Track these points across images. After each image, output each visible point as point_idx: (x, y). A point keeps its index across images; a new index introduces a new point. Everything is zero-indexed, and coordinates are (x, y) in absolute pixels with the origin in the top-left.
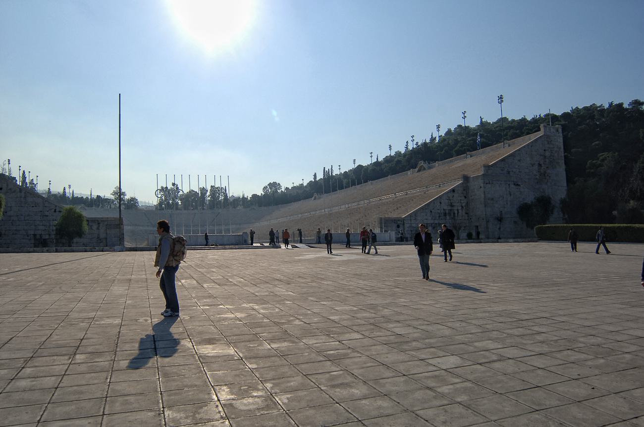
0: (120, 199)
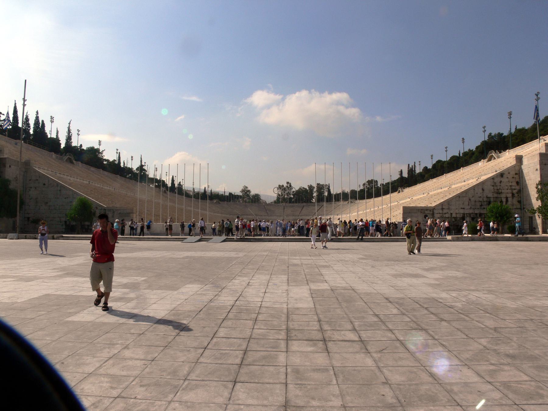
0: (248, 196)
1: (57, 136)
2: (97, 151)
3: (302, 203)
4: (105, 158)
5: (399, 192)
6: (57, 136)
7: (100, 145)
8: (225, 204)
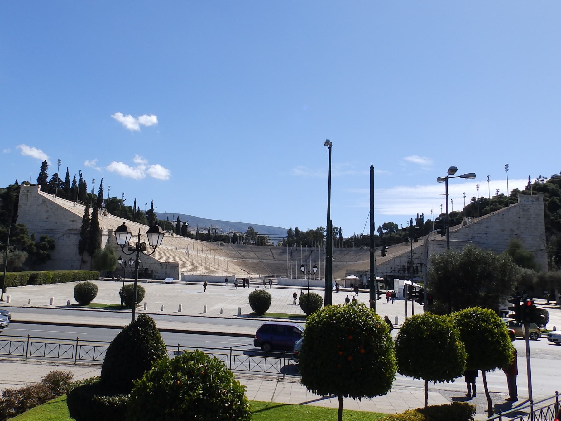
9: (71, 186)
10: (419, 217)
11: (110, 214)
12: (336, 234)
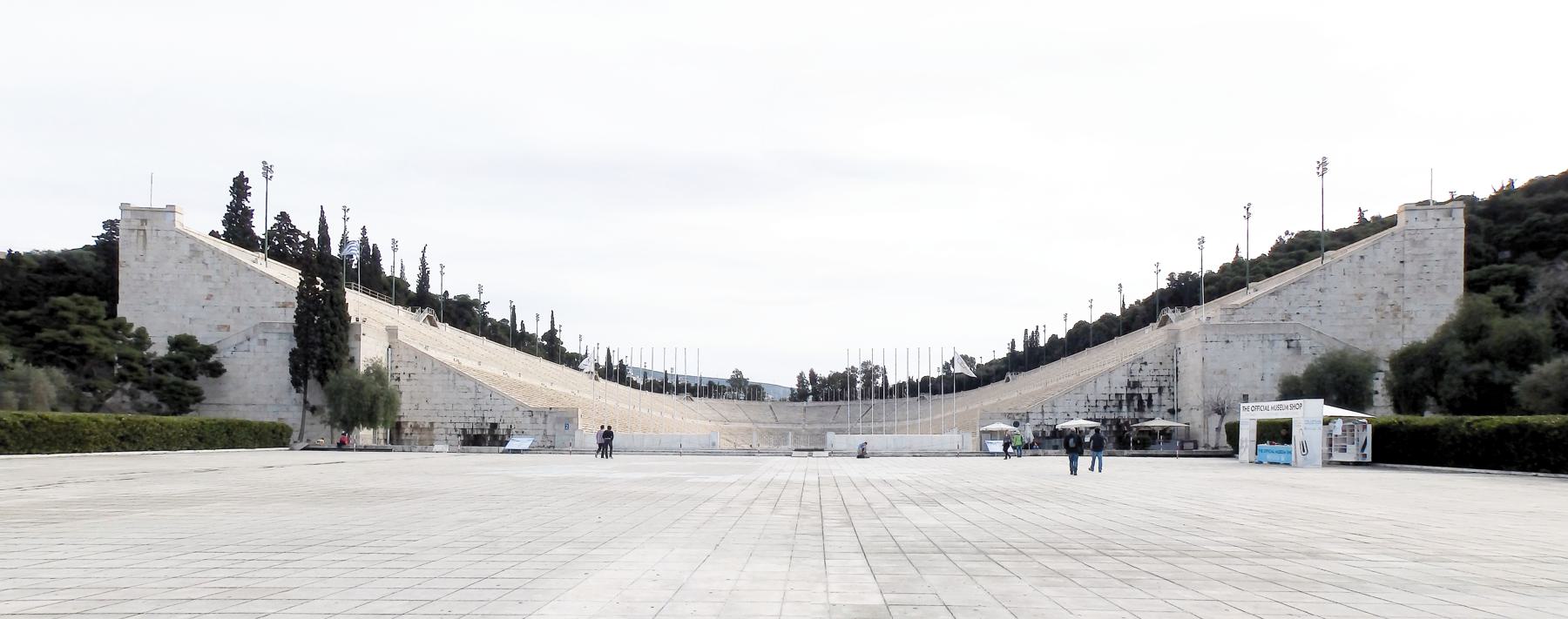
1: (402, 273)
2: (476, 303)
3: (836, 400)
4: (489, 316)
5: (1008, 380)
6: (402, 273)
7: (481, 293)
8: (700, 403)
9: (335, 252)
10: (1030, 334)
11: (447, 324)
12: (877, 376)
